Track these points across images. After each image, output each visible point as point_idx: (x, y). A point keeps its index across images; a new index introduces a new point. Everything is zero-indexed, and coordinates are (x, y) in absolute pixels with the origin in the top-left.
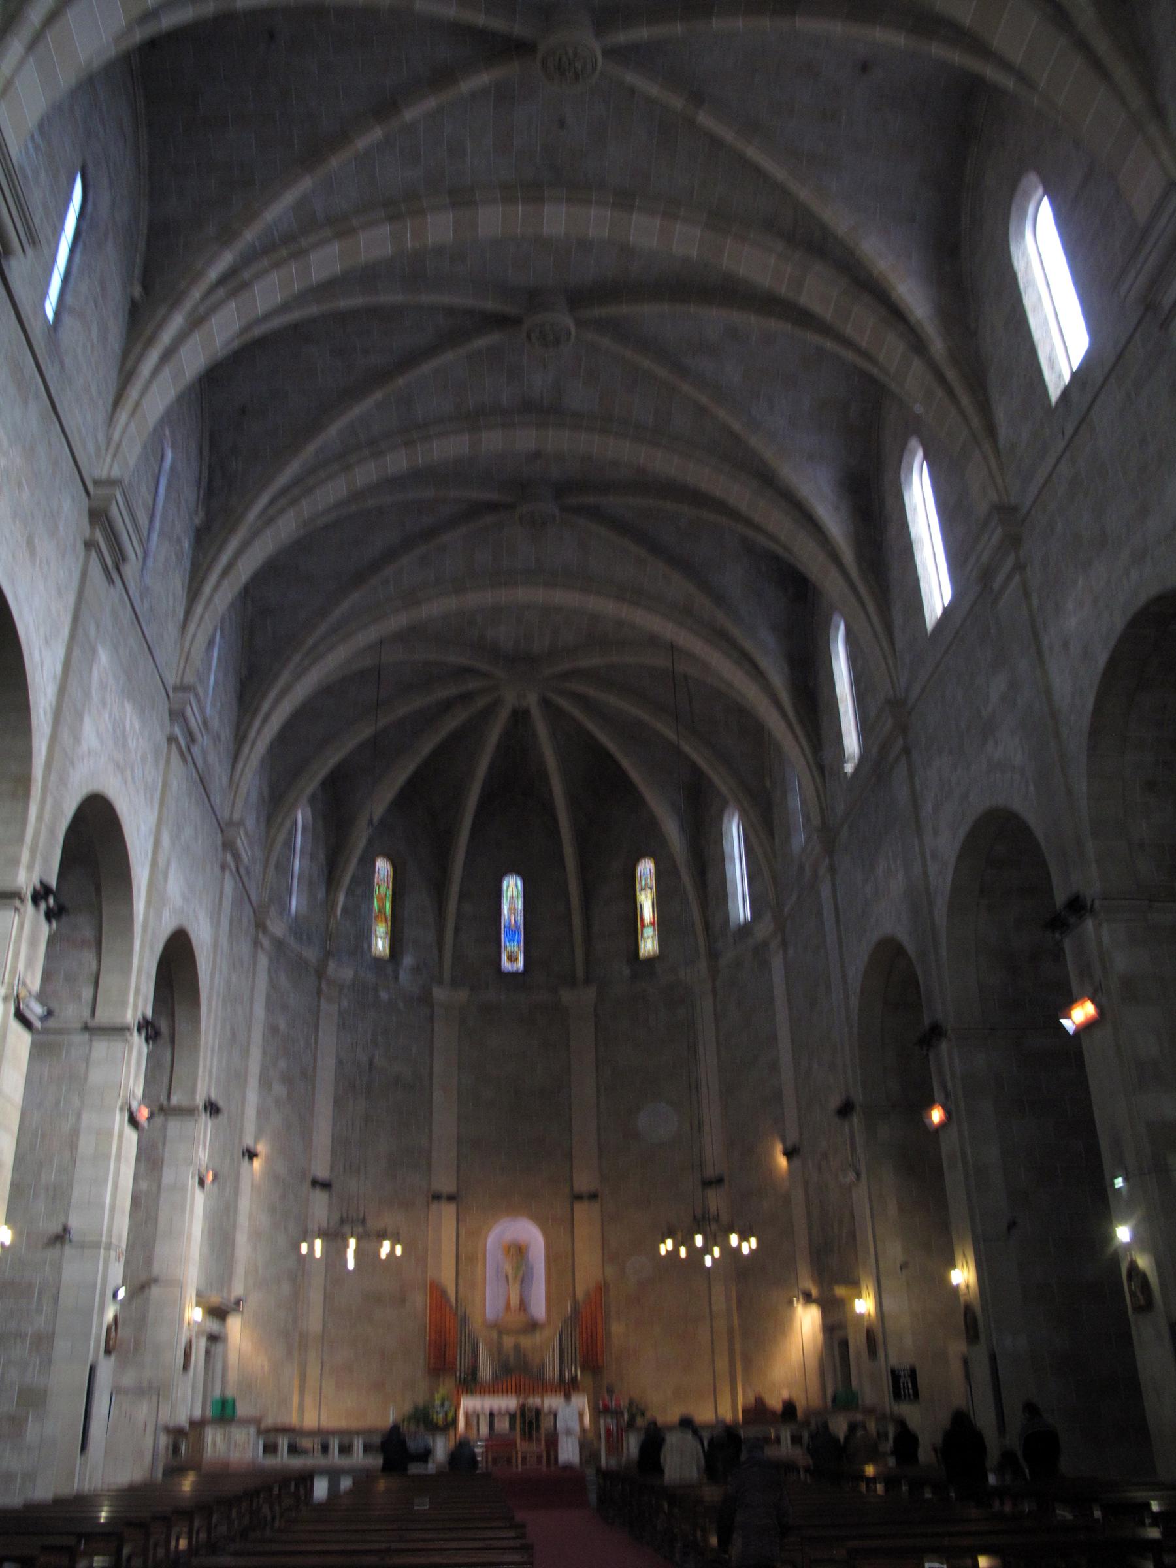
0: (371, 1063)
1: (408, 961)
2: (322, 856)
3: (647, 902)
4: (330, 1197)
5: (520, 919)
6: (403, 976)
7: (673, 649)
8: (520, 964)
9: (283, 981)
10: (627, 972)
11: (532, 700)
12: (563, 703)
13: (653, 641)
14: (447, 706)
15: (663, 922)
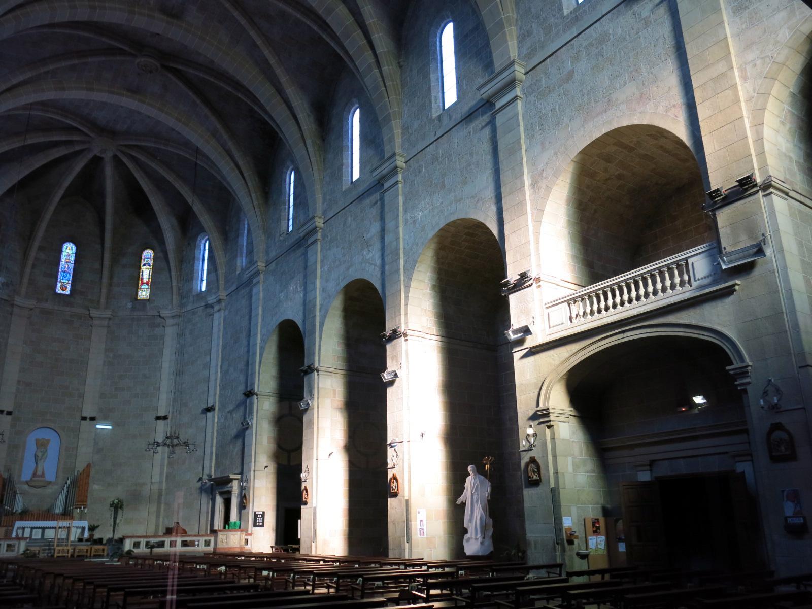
3: (146, 273)
5: (71, 266)
7: (197, 151)
8: (67, 292)
10: (130, 305)
11: (108, 156)
12: (125, 160)
13: (187, 144)
14: (56, 144)
15: (154, 284)
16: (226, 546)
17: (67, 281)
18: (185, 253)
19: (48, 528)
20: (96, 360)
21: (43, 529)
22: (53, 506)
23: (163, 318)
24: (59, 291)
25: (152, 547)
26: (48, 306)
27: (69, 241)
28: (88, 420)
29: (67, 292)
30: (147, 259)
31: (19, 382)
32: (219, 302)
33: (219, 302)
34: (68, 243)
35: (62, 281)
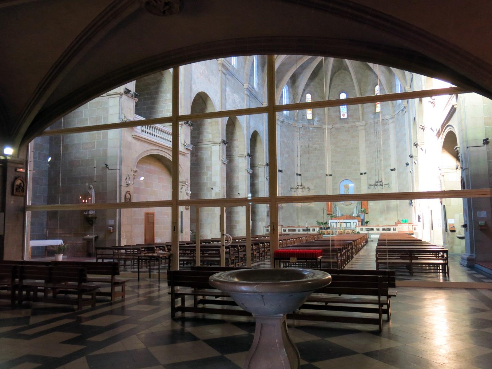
0: (309, 145)
1: (316, 119)
2: (292, 97)
4: (301, 178)
6: (315, 123)
8: (346, 117)
9: (285, 130)
10: (373, 116)
16: (402, 231)
17: (345, 112)
18: (392, 83)
19: (348, 222)
20: (363, 146)
21: (346, 223)
22: (352, 213)
23: (387, 120)
24: (342, 117)
25: (368, 231)
26: (338, 125)
27: (342, 93)
28: (363, 174)
29: (346, 117)
30: (377, 90)
31: (332, 162)
32: (405, 108)
33: (405, 108)
34: (343, 93)
35: (342, 112)
